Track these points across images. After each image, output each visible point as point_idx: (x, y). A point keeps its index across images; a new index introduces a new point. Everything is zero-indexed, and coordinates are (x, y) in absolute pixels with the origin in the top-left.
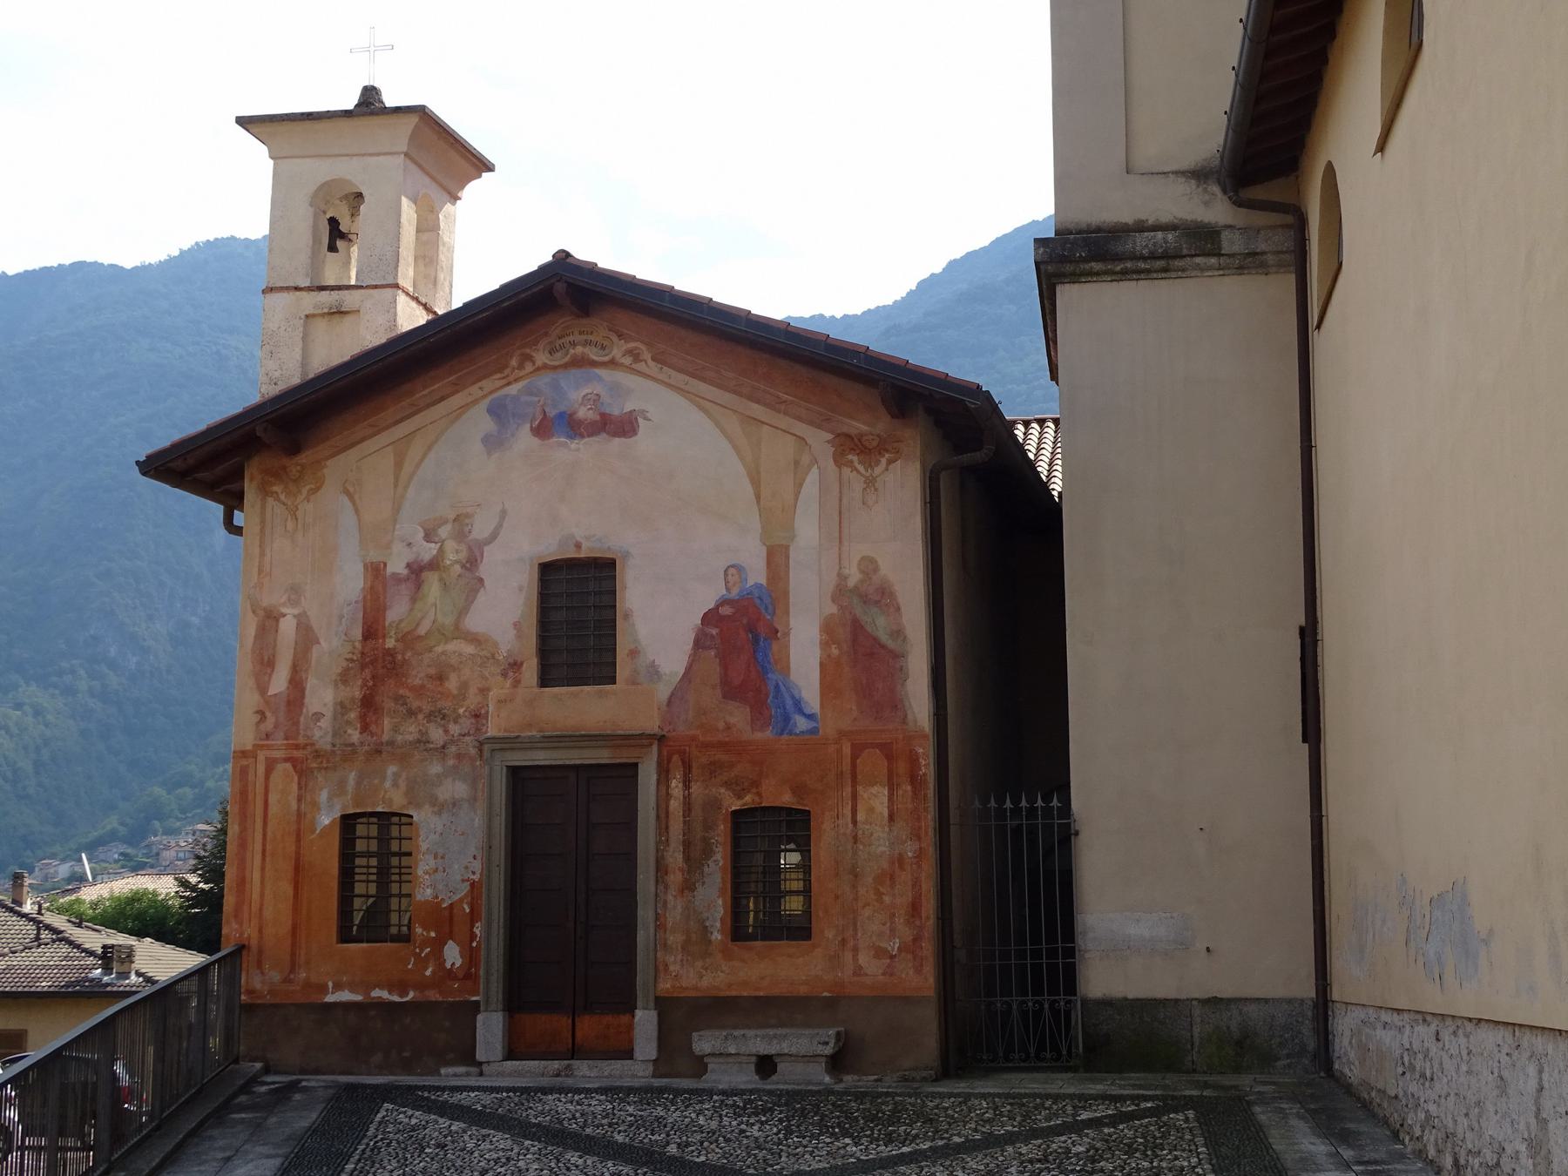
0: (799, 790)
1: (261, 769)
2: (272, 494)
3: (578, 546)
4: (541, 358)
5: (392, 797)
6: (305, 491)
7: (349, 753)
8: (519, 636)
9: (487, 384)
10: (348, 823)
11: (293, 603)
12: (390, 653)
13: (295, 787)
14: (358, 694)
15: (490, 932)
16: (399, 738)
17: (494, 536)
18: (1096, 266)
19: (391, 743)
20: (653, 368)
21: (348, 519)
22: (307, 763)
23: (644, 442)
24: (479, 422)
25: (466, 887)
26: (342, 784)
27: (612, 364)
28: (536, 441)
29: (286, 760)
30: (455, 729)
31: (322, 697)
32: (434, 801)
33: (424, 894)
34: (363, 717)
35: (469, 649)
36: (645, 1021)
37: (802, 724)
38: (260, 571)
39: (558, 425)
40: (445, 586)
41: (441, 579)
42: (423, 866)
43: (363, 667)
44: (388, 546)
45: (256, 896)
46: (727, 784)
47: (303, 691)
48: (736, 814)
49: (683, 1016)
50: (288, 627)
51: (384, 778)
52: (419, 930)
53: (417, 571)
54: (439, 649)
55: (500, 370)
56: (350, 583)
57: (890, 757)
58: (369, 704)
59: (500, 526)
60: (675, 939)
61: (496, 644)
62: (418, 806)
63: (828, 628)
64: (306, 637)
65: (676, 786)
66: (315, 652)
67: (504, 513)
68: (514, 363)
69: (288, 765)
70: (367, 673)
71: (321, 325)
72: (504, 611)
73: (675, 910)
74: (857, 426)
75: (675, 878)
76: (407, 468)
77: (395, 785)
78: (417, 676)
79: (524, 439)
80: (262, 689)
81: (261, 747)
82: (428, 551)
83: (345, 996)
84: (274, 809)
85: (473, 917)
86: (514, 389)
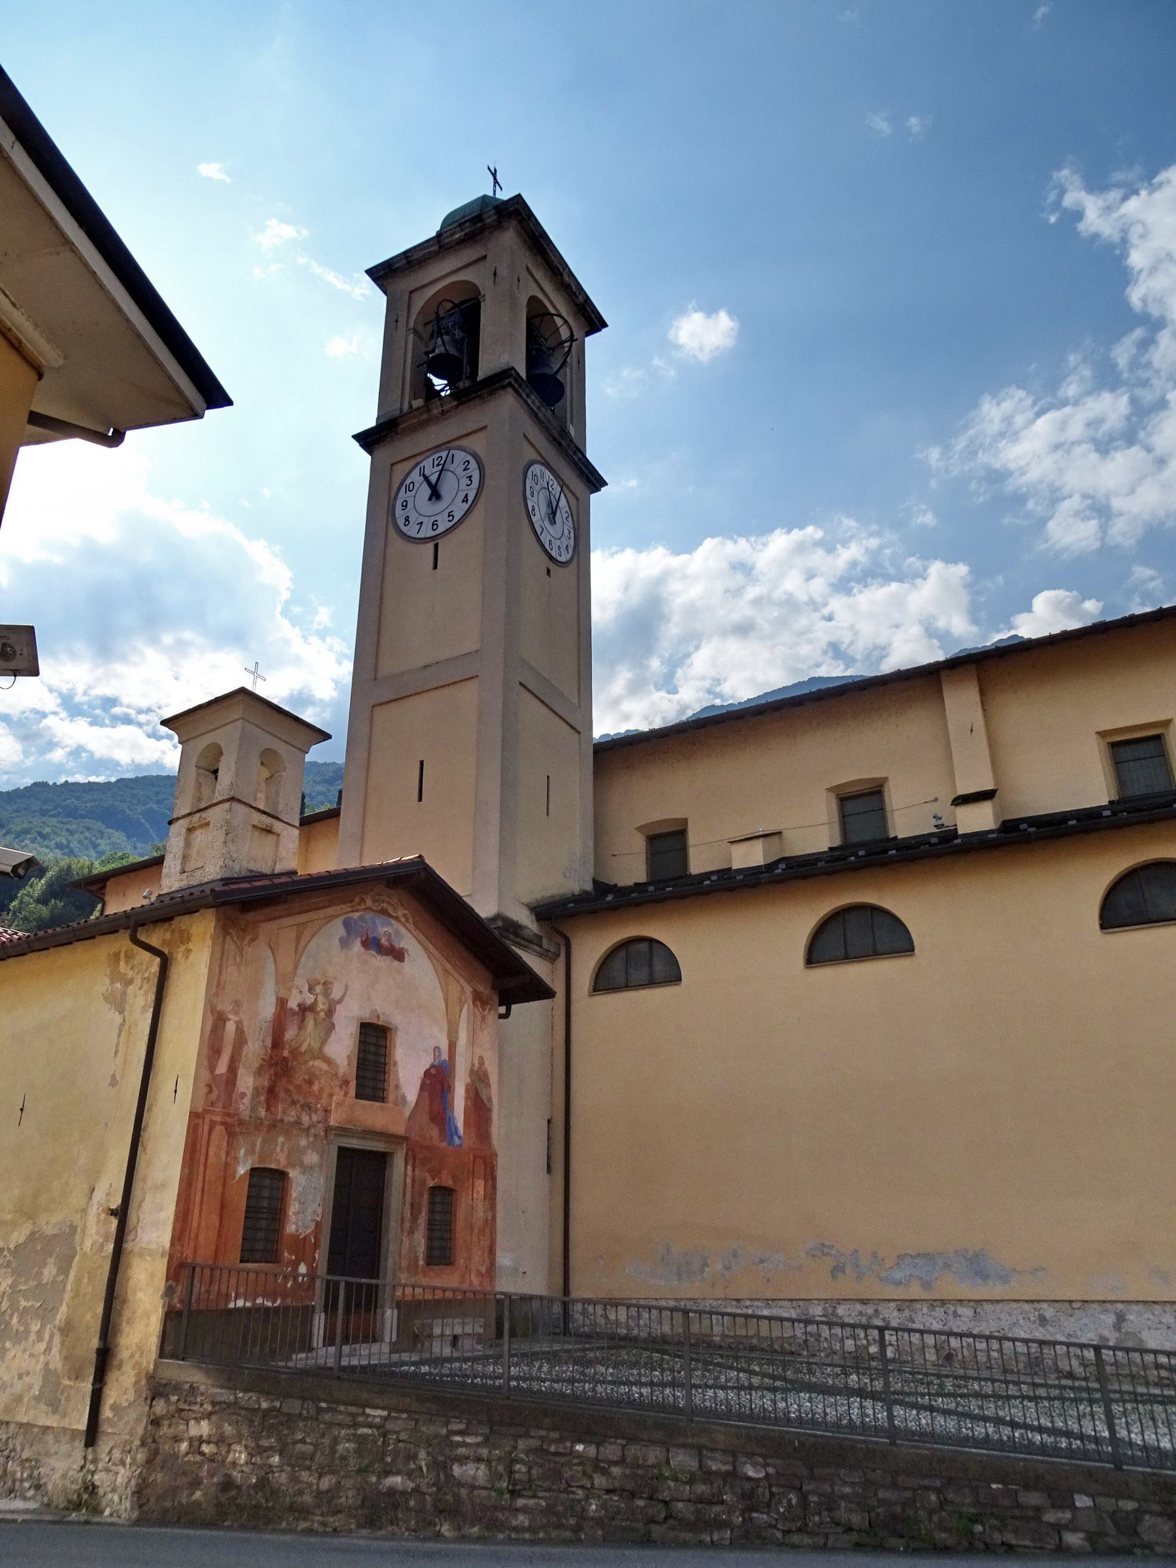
0: (455, 1178)
1: (206, 1128)
2: (230, 934)
3: (378, 1017)
4: (369, 903)
5: (278, 1160)
6: (247, 940)
7: (258, 1124)
8: (349, 1065)
9: (346, 908)
10: (254, 1171)
11: (236, 1013)
12: (285, 1059)
13: (225, 1144)
14: (266, 1084)
15: (321, 1256)
16: (286, 1119)
17: (340, 1001)
18: (512, 937)
19: (282, 1121)
20: (411, 927)
21: (270, 967)
22: (234, 1129)
23: (407, 966)
24: (337, 929)
25: (313, 1226)
26: (254, 1145)
27: (397, 918)
28: (362, 949)
29: (223, 1123)
30: (315, 1118)
31: (246, 1082)
32: (301, 1165)
33: (291, 1228)
34: (268, 1101)
35: (325, 1067)
36: (390, 1316)
37: (457, 1141)
38: (218, 985)
39: (372, 944)
40: (316, 1024)
41: (315, 1019)
42: (293, 1208)
43: (271, 1066)
44: (290, 990)
45: (195, 1224)
46: (429, 1171)
47: (236, 1076)
48: (433, 1188)
49: (410, 1309)
50: (231, 1027)
51: (276, 1145)
52: (286, 1254)
53: (304, 1009)
54: (311, 1063)
55: (351, 901)
56: (267, 1008)
57: (485, 1163)
58: (271, 1092)
59: (345, 994)
60: (404, 1263)
61: (338, 1067)
62: (294, 1166)
63: (467, 1091)
64: (241, 1040)
65: (409, 1168)
66: (245, 1050)
67: (347, 987)
68: (357, 900)
69: (223, 1127)
70: (272, 1070)
71: (257, 834)
72: (342, 1047)
73: (406, 1241)
74: (481, 989)
75: (407, 1225)
76: (302, 943)
77: (282, 1150)
78: (299, 1077)
79: (357, 947)
80: (212, 1068)
81: (209, 1112)
82: (309, 999)
83: (240, 1303)
84: (211, 1159)
85: (316, 1245)
86: (356, 915)
